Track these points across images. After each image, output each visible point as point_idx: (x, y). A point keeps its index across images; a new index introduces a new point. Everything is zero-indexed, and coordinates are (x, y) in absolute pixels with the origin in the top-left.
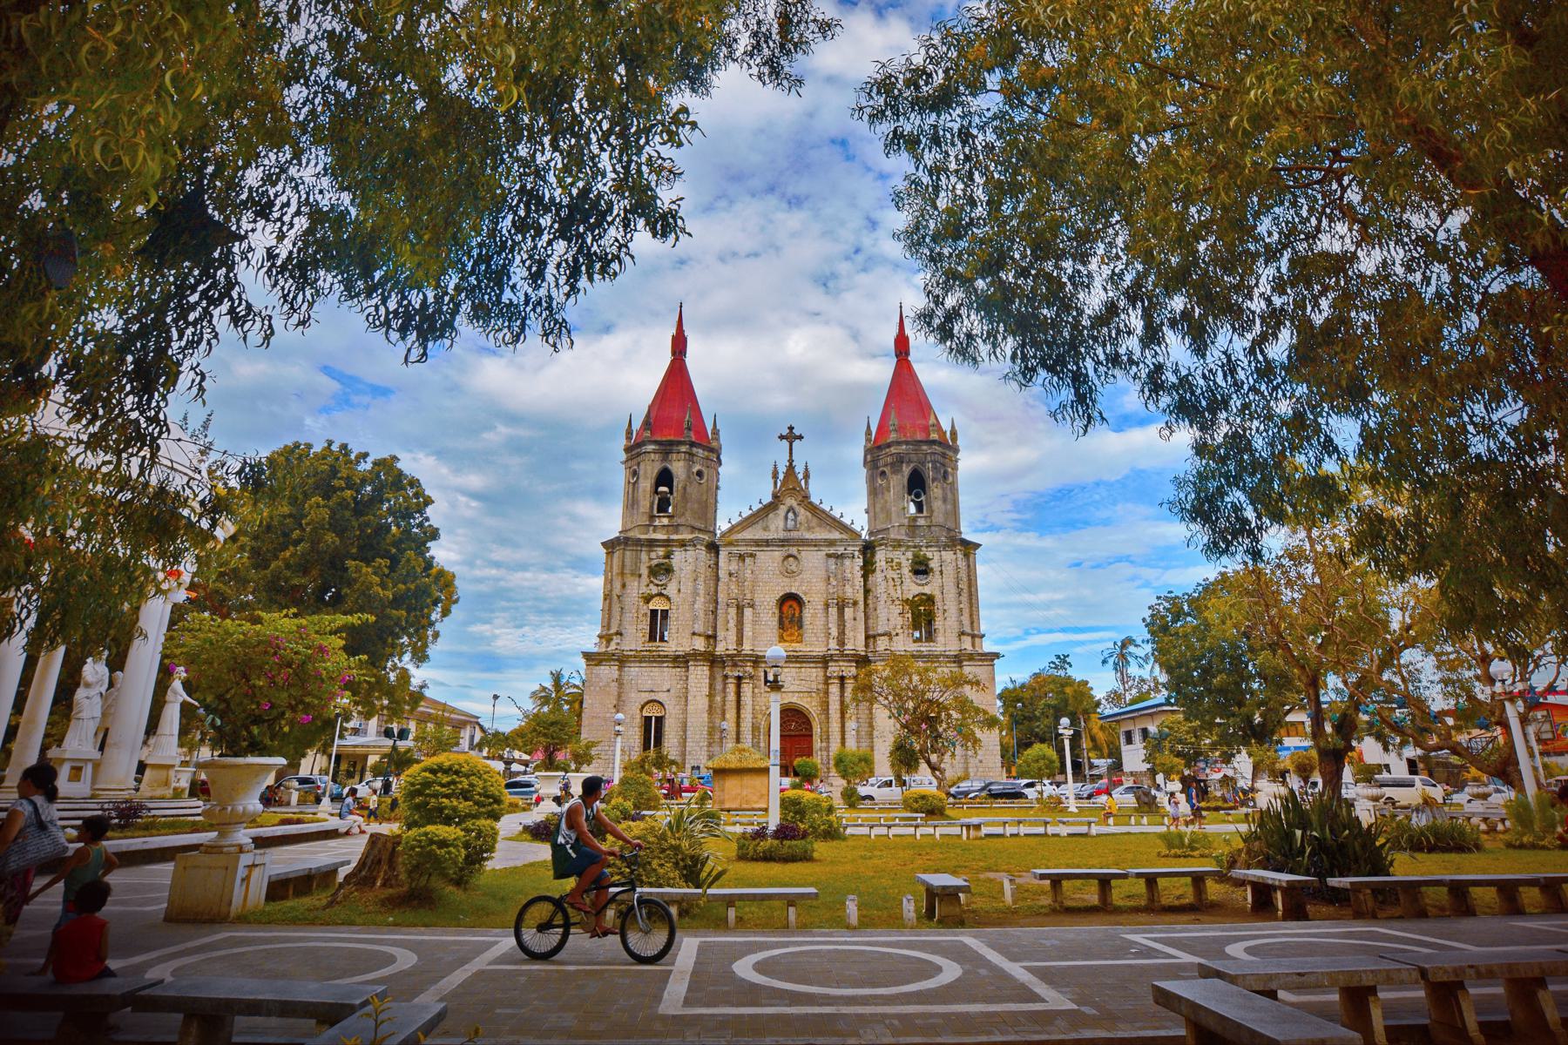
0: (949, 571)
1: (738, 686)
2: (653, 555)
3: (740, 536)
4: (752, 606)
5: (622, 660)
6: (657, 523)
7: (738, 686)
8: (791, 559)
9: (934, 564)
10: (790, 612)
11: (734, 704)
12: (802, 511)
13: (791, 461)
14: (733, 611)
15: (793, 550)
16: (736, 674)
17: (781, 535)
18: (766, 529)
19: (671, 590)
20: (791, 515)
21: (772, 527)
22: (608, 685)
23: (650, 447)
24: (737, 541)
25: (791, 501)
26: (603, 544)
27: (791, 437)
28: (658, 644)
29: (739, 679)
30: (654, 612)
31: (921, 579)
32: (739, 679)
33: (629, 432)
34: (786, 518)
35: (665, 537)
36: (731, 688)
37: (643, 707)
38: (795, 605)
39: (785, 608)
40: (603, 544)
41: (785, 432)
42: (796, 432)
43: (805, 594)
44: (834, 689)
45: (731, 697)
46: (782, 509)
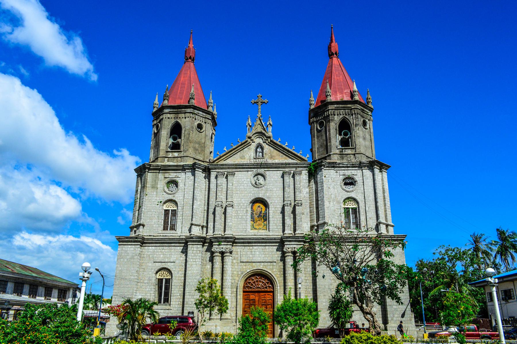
0: (369, 182)
2: (167, 175)
3: (224, 162)
5: (143, 242)
8: (259, 176)
9: (356, 178)
10: (259, 210)
12: (267, 146)
14: (219, 211)
15: (261, 171)
17: (253, 161)
18: (242, 158)
19: (178, 197)
21: (247, 157)
22: (133, 257)
24: (222, 165)
28: (169, 231)
31: (350, 188)
32: (222, 253)
34: (256, 152)
35: (175, 164)
36: (218, 259)
37: (157, 273)
38: (262, 206)
43: (269, 198)
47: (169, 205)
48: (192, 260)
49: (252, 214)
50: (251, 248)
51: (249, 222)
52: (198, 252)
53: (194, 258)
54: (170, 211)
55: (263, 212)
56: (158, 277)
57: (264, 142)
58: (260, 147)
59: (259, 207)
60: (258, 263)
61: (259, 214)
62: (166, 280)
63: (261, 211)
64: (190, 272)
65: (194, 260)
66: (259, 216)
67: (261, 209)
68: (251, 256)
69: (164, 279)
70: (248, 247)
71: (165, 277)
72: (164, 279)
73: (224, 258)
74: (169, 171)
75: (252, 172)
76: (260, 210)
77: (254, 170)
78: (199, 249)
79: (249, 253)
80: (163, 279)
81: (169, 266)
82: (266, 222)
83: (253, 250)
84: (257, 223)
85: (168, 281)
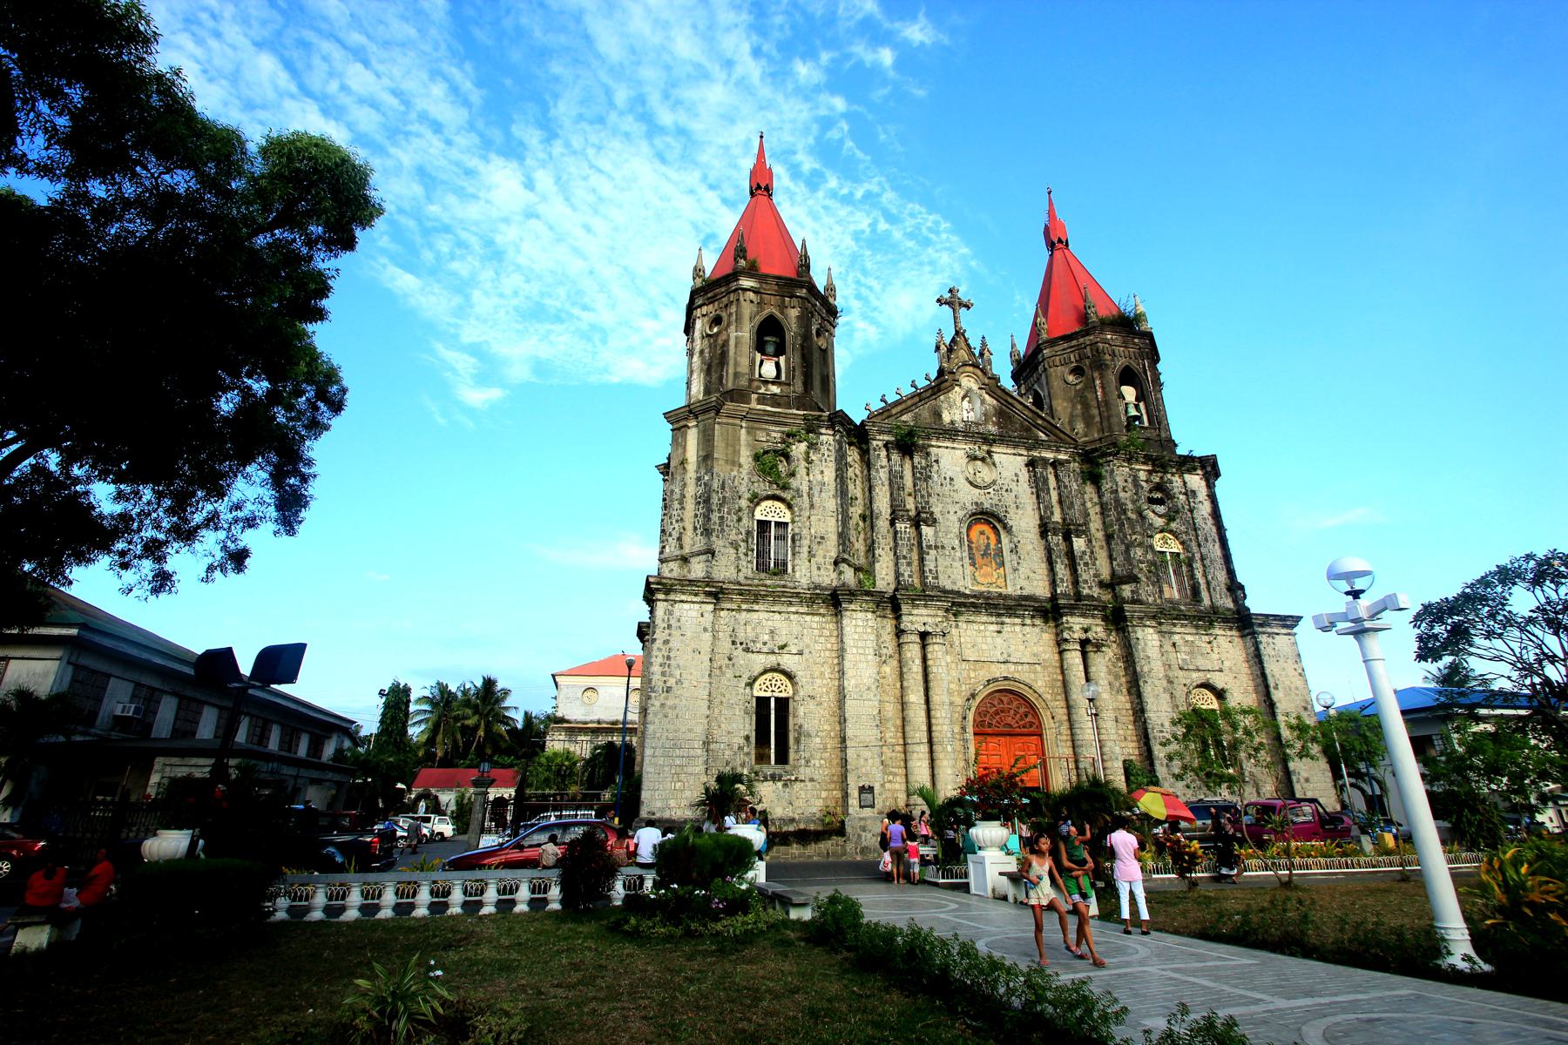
1: (924, 647)
4: (932, 522)
6: (762, 391)
7: (924, 647)
10: (983, 541)
11: (920, 677)
13: (959, 333)
16: (922, 629)
20: (965, 403)
23: (746, 283)
25: (968, 382)
26: (667, 415)
27: (952, 301)
29: (924, 636)
30: (764, 525)
32: (924, 636)
33: (698, 271)
36: (913, 651)
38: (986, 528)
39: (974, 533)
40: (667, 415)
41: (947, 296)
42: (963, 295)
44: (1074, 658)
45: (916, 667)
46: (957, 393)
47: (768, 510)
48: (854, 651)
49: (970, 548)
50: (982, 627)
51: (969, 569)
52: (869, 630)
53: (860, 644)
54: (773, 524)
55: (992, 546)
56: (757, 693)
57: (980, 388)
58: (967, 399)
59: (982, 533)
60: (1002, 665)
61: (985, 551)
62: (777, 699)
63: (988, 545)
64: (853, 682)
65: (862, 651)
66: (985, 555)
67: (988, 538)
68: (985, 647)
69: (773, 700)
70: (976, 627)
71: (776, 694)
72: (773, 700)
73: (930, 649)
74: (764, 426)
75: (963, 451)
76: (986, 541)
77: (967, 447)
78: (870, 624)
79: (980, 640)
80: (769, 698)
81: (788, 662)
82: (1002, 569)
83: (988, 634)
84: (982, 571)
85: (783, 704)
